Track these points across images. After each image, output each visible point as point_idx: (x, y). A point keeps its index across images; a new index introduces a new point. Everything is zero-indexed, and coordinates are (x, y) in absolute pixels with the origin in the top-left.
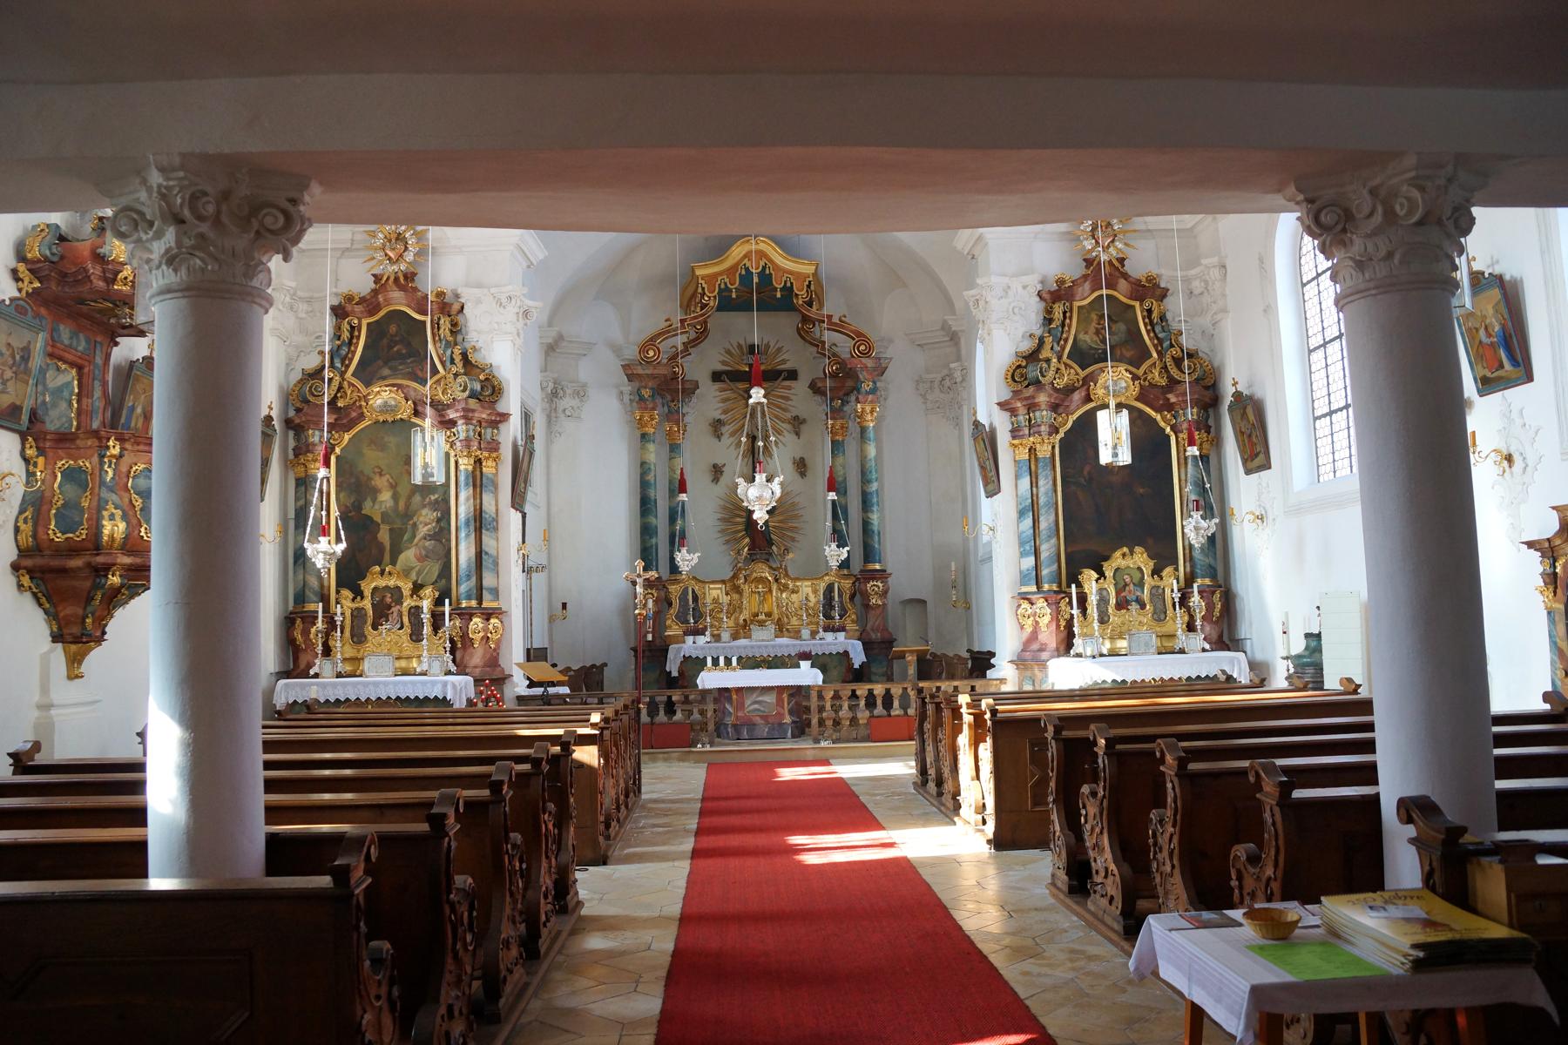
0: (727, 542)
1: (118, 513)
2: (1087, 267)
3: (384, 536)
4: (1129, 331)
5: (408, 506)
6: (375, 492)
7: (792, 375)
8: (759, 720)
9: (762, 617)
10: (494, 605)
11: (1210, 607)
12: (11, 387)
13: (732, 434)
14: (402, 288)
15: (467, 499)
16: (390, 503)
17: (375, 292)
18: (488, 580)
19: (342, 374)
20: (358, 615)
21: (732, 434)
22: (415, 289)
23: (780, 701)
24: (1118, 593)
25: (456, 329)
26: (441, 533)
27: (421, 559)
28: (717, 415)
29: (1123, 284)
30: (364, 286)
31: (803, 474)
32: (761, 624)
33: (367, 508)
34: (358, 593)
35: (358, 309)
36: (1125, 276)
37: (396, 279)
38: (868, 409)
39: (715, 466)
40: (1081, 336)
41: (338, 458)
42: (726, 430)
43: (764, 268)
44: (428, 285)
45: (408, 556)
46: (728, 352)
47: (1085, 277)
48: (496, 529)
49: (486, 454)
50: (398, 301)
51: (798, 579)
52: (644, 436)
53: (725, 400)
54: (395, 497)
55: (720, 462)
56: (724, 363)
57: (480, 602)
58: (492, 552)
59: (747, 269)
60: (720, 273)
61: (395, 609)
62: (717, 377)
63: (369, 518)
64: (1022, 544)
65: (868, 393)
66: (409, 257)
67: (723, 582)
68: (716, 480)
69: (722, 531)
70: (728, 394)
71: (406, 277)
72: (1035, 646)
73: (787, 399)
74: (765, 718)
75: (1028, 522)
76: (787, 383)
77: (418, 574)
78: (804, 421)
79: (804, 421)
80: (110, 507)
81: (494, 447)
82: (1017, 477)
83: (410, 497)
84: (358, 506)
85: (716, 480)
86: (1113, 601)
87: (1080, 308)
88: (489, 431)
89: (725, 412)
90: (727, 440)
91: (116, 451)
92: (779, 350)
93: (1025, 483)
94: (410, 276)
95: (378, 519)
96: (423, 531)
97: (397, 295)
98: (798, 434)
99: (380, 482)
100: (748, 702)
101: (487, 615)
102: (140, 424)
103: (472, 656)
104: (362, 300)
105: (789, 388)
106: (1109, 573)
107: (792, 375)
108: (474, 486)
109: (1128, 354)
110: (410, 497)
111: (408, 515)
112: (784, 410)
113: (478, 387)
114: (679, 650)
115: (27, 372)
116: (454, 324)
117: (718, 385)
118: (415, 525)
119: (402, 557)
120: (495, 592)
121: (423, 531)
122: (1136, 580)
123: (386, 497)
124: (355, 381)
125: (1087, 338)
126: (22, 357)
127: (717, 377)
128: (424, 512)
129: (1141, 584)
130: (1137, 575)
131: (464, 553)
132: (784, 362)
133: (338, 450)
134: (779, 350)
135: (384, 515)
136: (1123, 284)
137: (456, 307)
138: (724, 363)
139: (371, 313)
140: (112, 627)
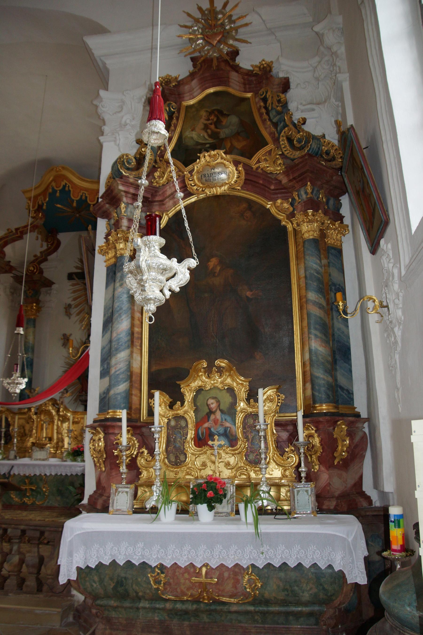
2: (194, 66)
4: (242, 123)
11: (330, 444)
13: (78, 314)
21: (78, 314)
24: (198, 425)
28: (69, 301)
29: (234, 76)
36: (236, 68)
39: (64, 335)
40: (188, 134)
42: (74, 311)
47: (192, 75)
53: (74, 292)
55: (68, 333)
56: (77, 268)
59: (53, 188)
62: (70, 276)
70: (77, 287)
86: (191, 434)
87: (188, 107)
89: (75, 299)
90: (74, 318)
106: (189, 396)
109: (239, 145)
122: (225, 406)
125: (194, 135)
129: (231, 411)
130: (227, 399)
136: (234, 76)
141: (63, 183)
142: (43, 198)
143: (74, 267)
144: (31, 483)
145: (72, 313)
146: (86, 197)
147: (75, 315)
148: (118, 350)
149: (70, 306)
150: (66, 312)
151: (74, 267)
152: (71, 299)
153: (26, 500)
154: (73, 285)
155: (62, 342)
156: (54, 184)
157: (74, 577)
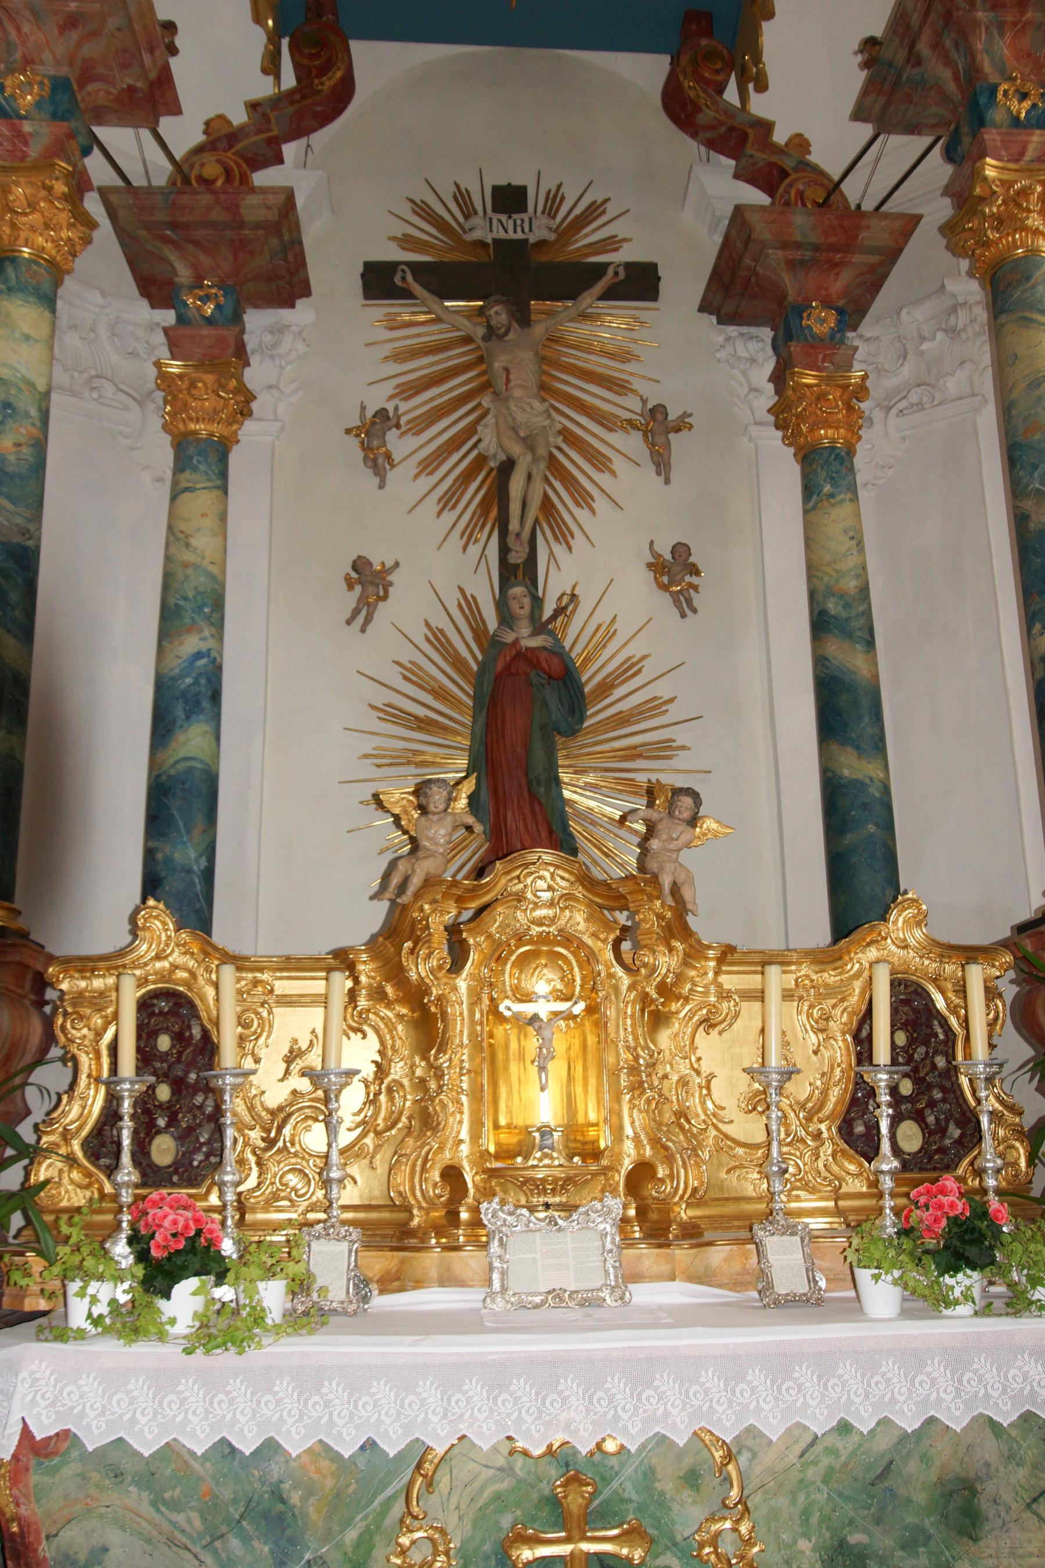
9: (545, 1165)
13: (428, 465)
21: (428, 465)
28: (377, 399)
31: (685, 604)
32: (560, 1197)
39: (360, 565)
46: (423, 210)
51: (727, 954)
56: (407, 242)
67: (342, 960)
68: (363, 613)
79: (682, 425)
85: (363, 613)
89: (409, 390)
90: (406, 483)
92: (595, 210)
117: (381, 309)
132: (611, 244)
134: (595, 210)
138: (407, 242)
143: (394, 239)
145: (397, 457)
147: (410, 467)
150: (366, 448)
151: (394, 239)
152: (389, 388)
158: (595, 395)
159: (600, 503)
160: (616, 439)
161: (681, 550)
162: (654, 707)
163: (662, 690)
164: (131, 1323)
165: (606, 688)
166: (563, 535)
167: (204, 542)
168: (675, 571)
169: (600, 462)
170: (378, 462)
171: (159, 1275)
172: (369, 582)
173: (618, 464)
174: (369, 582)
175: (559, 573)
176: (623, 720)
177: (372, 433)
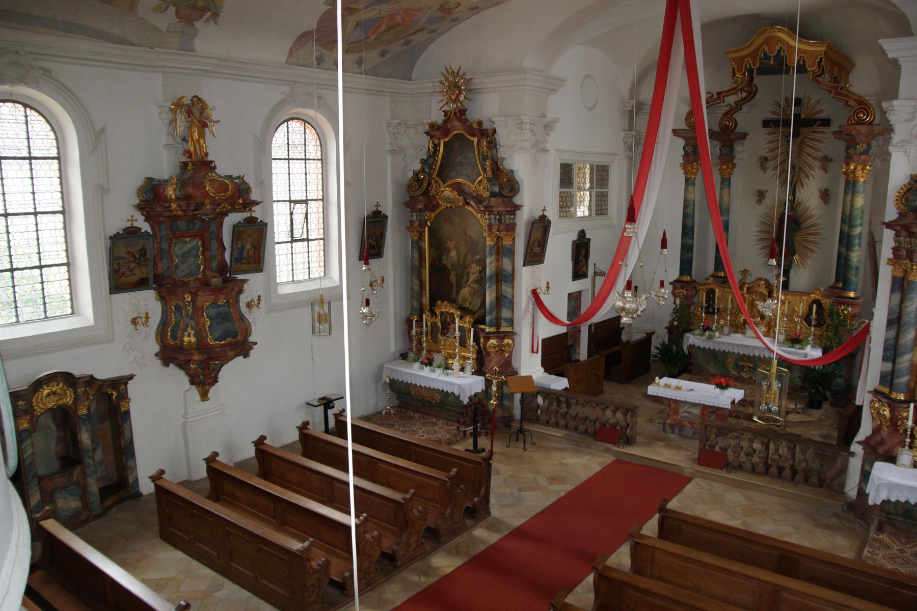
0: (763, 248)
1: (193, 332)
3: (453, 278)
5: (464, 261)
6: (448, 251)
7: (826, 122)
8: (687, 424)
10: (509, 329)
12: (136, 271)
14: (460, 120)
15: (491, 263)
16: (456, 259)
17: (445, 122)
18: (505, 314)
19: (430, 175)
20: (434, 325)
22: (466, 120)
23: (702, 414)
25: (493, 144)
26: (481, 281)
27: (471, 295)
28: (764, 153)
30: (438, 117)
33: (444, 261)
34: (433, 314)
35: (437, 133)
37: (455, 113)
38: (859, 167)
41: (429, 227)
42: (770, 164)
43: (779, 51)
44: (473, 116)
45: (465, 292)
48: (513, 281)
49: (504, 233)
50: (458, 129)
52: (687, 180)
53: (771, 142)
54: (458, 254)
55: (763, 188)
56: (774, 113)
57: (498, 326)
58: (510, 296)
59: (765, 53)
60: (747, 56)
61: (452, 326)
62: (766, 124)
63: (446, 266)
64: (886, 349)
65: (861, 154)
66: (462, 98)
68: (759, 201)
69: (761, 240)
71: (460, 111)
72: (879, 437)
73: (820, 141)
74: (692, 423)
75: (893, 333)
76: (821, 129)
77: (470, 304)
78: (831, 160)
79: (831, 160)
80: (189, 330)
81: (512, 228)
82: (892, 291)
83: (465, 256)
84: (440, 259)
85: (759, 201)
88: (508, 216)
89: (771, 151)
90: (770, 172)
91: (189, 299)
93: (897, 297)
94: (463, 112)
95: (449, 267)
96: (473, 277)
97: (457, 123)
98: (825, 169)
99: (450, 244)
100: (681, 411)
101: (501, 336)
102: (251, 253)
103: (490, 361)
104: (439, 128)
105: (823, 133)
107: (826, 122)
108: (498, 253)
110: (465, 256)
111: (465, 267)
112: (817, 150)
113: (496, 189)
114: (688, 338)
115: (146, 260)
116: (490, 142)
118: (468, 273)
119: (462, 292)
120: (511, 322)
121: (473, 277)
123: (453, 254)
124: (438, 179)
126: (141, 255)
127: (766, 124)
128: (473, 265)
131: (490, 297)
132: (821, 111)
133: (429, 223)
135: (453, 265)
137: (490, 132)
138: (774, 113)
139: (446, 136)
140: (222, 375)
141: (778, 47)
142: (751, 62)
144: (749, 361)
146: (804, 62)
148: (905, 353)
149: (766, 159)
150: (762, 166)
152: (767, 150)
153: (743, 374)
154: (769, 134)
155: (756, 198)
156: (766, 49)
157: (879, 503)
158: (812, 152)
159: (811, 178)
160: (816, 163)
161: (827, 190)
162: (814, 225)
163: (818, 222)
164: (701, 335)
165: (806, 221)
166: (802, 186)
167: (726, 199)
168: (825, 196)
169: (812, 168)
170: (763, 168)
171: (704, 331)
172: (761, 196)
173: (816, 169)
174: (761, 196)
175: (801, 195)
176: (809, 227)
177: (764, 161)
